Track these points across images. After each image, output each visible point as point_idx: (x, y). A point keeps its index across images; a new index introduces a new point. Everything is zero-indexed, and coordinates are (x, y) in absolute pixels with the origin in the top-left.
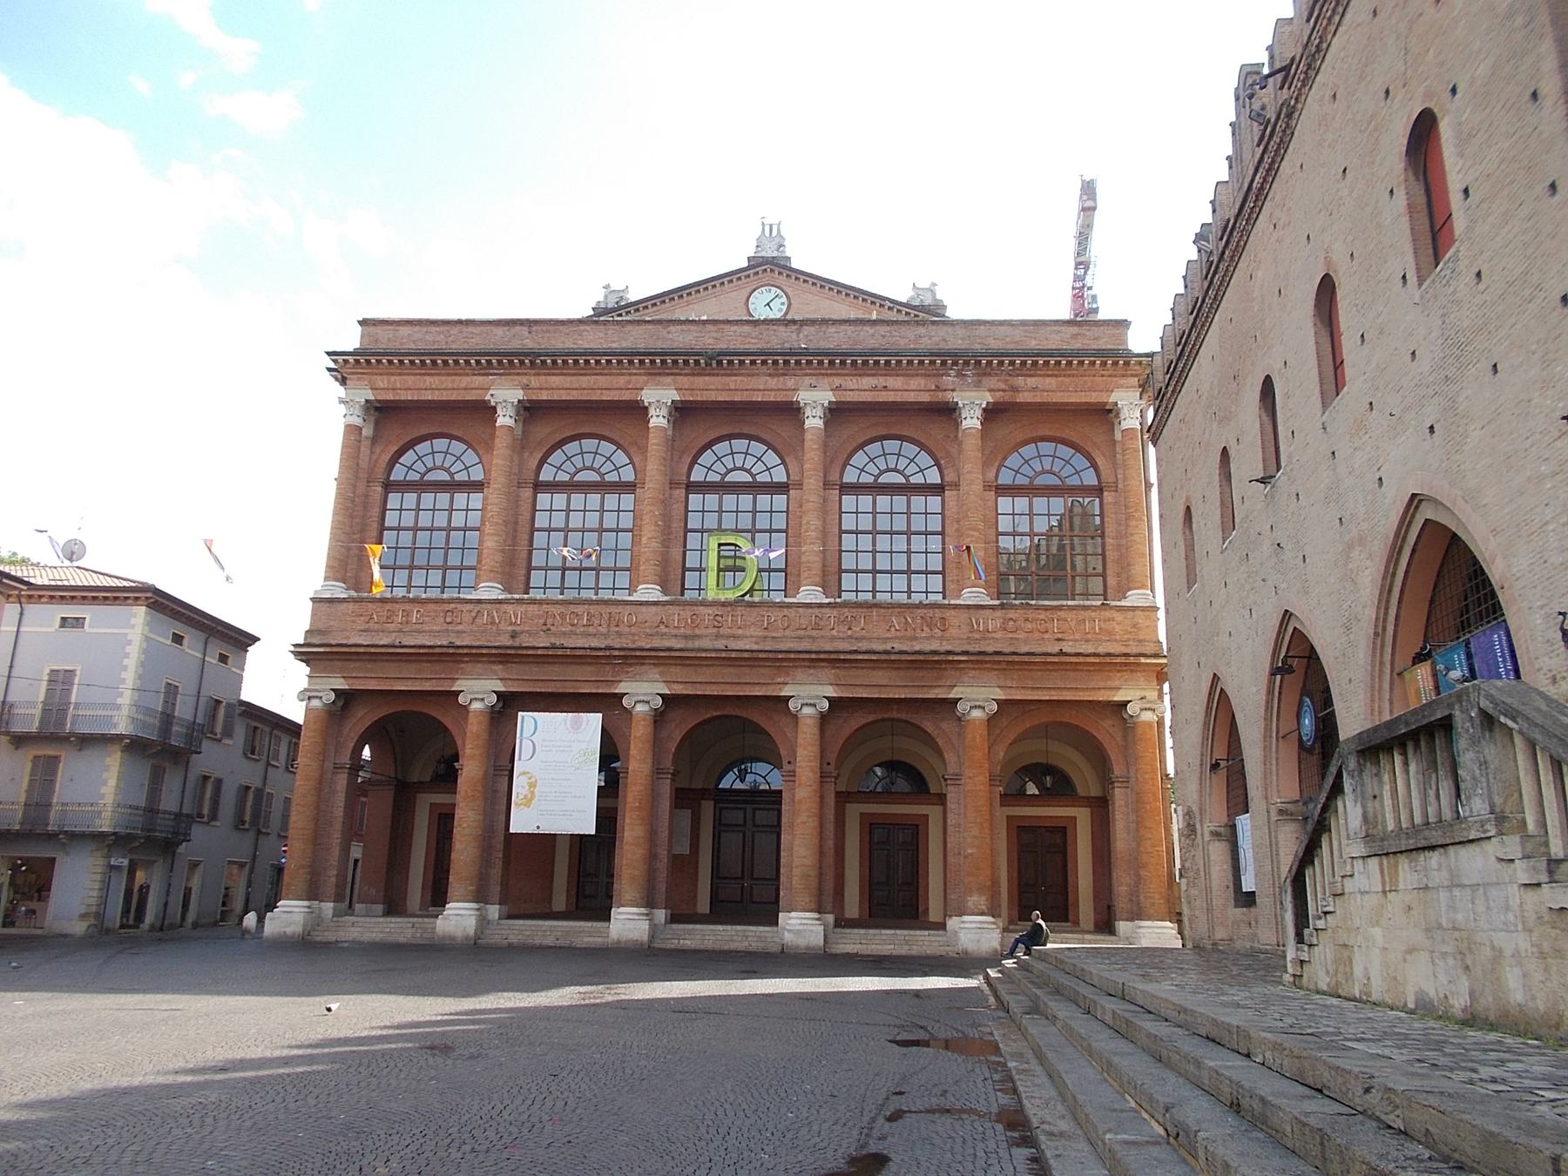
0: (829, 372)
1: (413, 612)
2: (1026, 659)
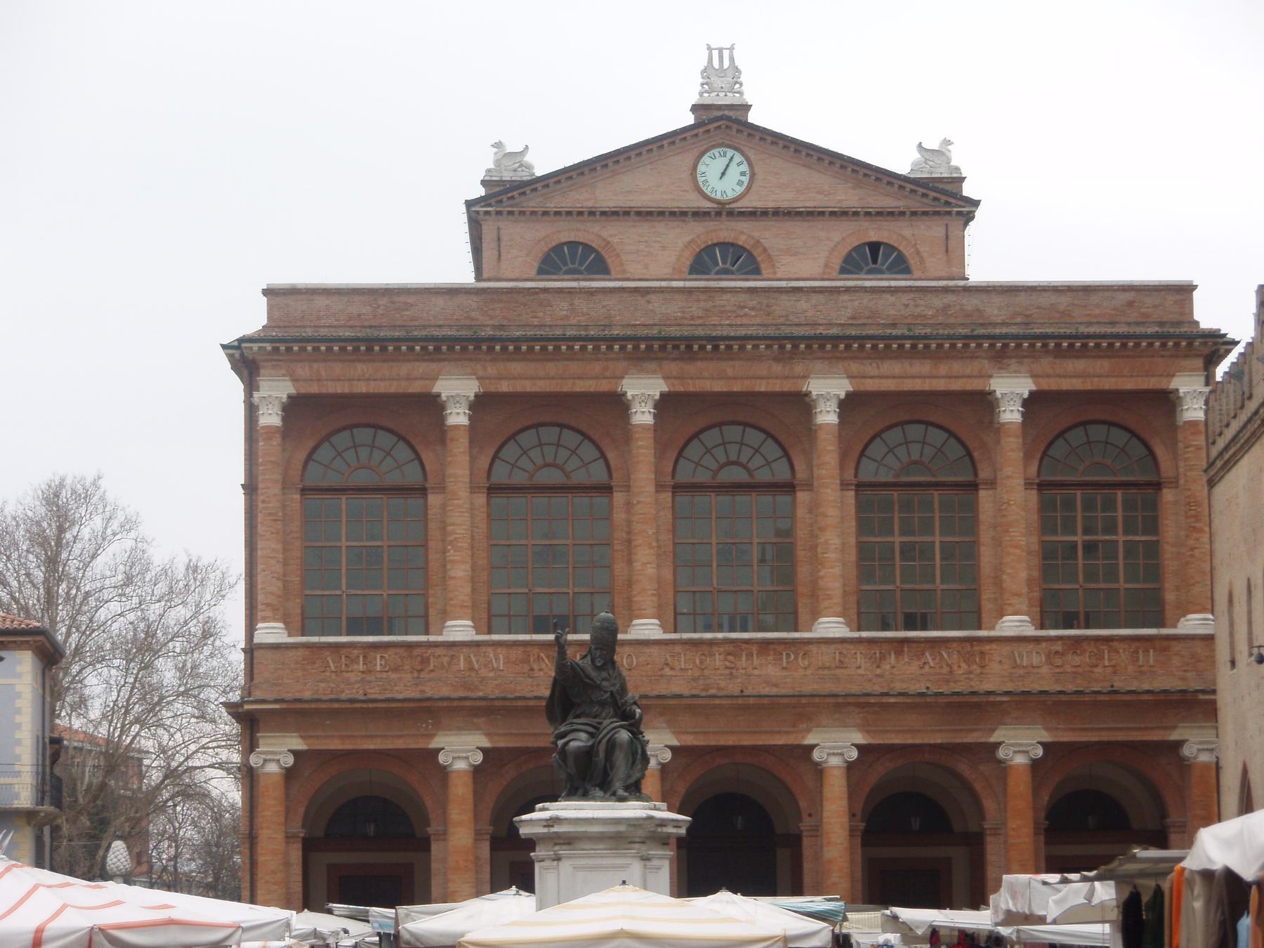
0: (845, 355)
1: (375, 659)
2: (1074, 698)
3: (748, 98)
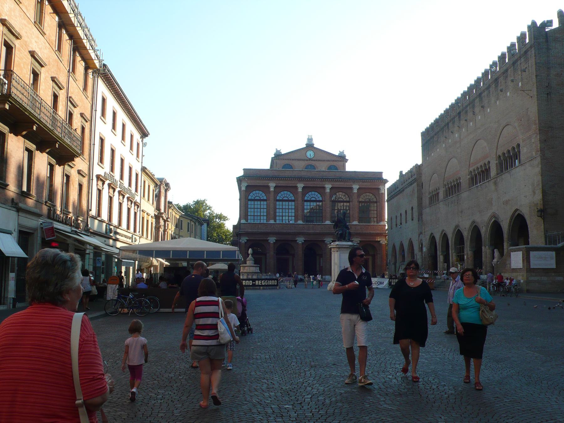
3: (314, 143)
